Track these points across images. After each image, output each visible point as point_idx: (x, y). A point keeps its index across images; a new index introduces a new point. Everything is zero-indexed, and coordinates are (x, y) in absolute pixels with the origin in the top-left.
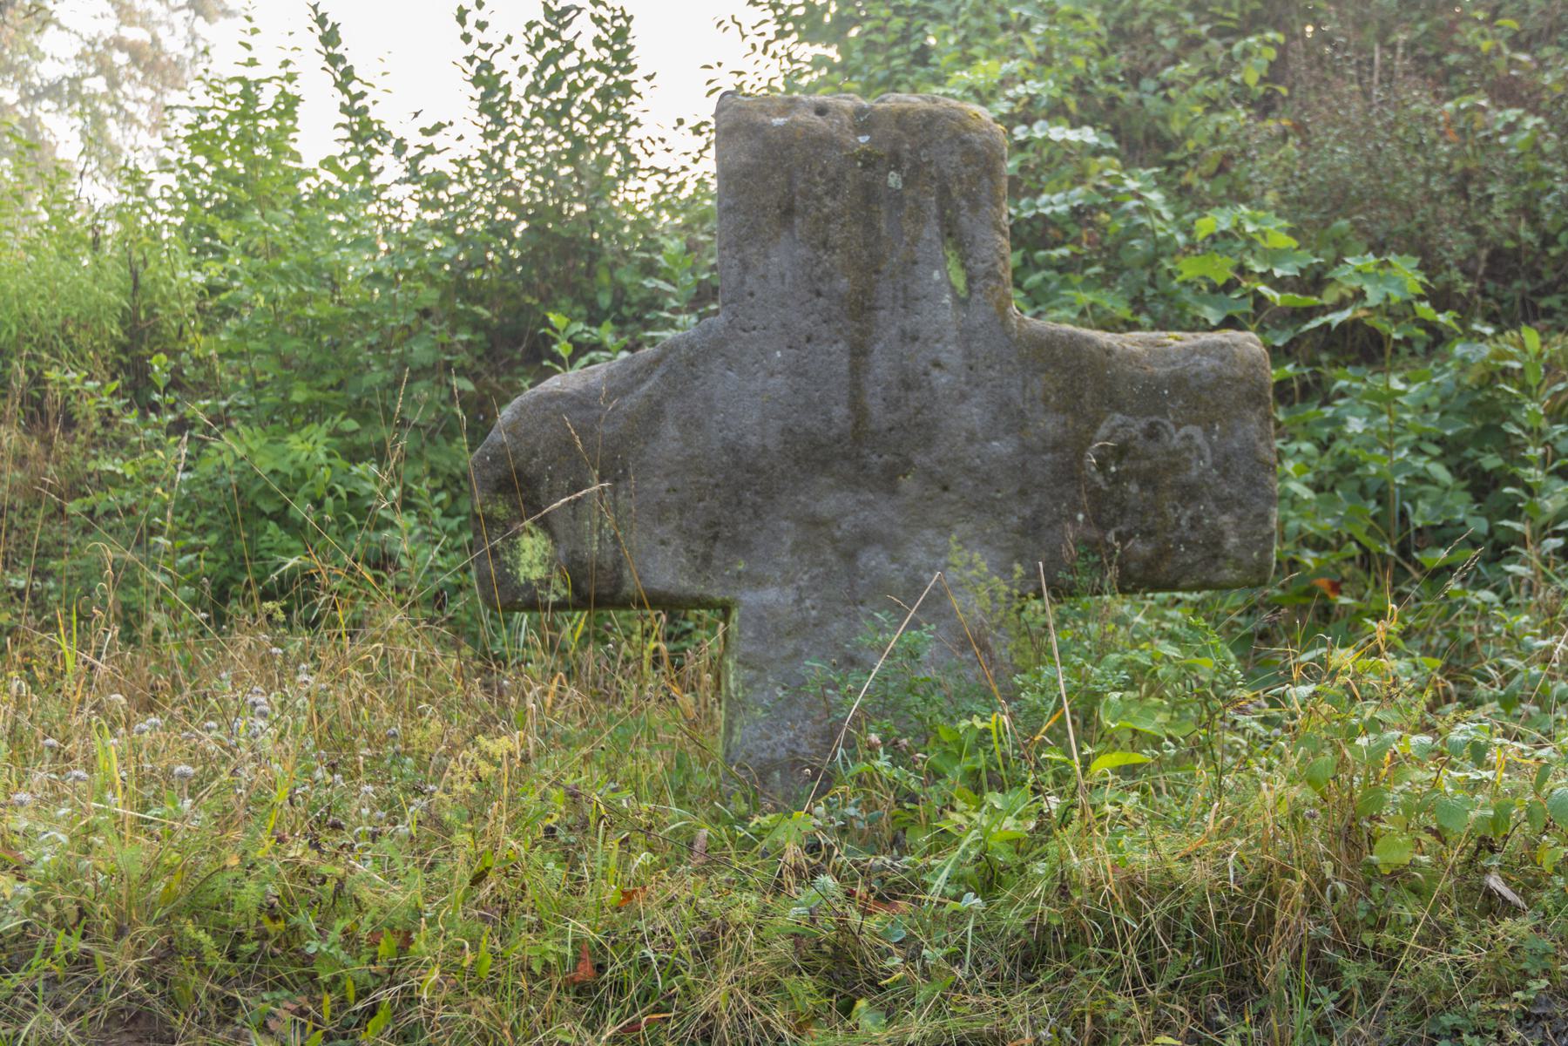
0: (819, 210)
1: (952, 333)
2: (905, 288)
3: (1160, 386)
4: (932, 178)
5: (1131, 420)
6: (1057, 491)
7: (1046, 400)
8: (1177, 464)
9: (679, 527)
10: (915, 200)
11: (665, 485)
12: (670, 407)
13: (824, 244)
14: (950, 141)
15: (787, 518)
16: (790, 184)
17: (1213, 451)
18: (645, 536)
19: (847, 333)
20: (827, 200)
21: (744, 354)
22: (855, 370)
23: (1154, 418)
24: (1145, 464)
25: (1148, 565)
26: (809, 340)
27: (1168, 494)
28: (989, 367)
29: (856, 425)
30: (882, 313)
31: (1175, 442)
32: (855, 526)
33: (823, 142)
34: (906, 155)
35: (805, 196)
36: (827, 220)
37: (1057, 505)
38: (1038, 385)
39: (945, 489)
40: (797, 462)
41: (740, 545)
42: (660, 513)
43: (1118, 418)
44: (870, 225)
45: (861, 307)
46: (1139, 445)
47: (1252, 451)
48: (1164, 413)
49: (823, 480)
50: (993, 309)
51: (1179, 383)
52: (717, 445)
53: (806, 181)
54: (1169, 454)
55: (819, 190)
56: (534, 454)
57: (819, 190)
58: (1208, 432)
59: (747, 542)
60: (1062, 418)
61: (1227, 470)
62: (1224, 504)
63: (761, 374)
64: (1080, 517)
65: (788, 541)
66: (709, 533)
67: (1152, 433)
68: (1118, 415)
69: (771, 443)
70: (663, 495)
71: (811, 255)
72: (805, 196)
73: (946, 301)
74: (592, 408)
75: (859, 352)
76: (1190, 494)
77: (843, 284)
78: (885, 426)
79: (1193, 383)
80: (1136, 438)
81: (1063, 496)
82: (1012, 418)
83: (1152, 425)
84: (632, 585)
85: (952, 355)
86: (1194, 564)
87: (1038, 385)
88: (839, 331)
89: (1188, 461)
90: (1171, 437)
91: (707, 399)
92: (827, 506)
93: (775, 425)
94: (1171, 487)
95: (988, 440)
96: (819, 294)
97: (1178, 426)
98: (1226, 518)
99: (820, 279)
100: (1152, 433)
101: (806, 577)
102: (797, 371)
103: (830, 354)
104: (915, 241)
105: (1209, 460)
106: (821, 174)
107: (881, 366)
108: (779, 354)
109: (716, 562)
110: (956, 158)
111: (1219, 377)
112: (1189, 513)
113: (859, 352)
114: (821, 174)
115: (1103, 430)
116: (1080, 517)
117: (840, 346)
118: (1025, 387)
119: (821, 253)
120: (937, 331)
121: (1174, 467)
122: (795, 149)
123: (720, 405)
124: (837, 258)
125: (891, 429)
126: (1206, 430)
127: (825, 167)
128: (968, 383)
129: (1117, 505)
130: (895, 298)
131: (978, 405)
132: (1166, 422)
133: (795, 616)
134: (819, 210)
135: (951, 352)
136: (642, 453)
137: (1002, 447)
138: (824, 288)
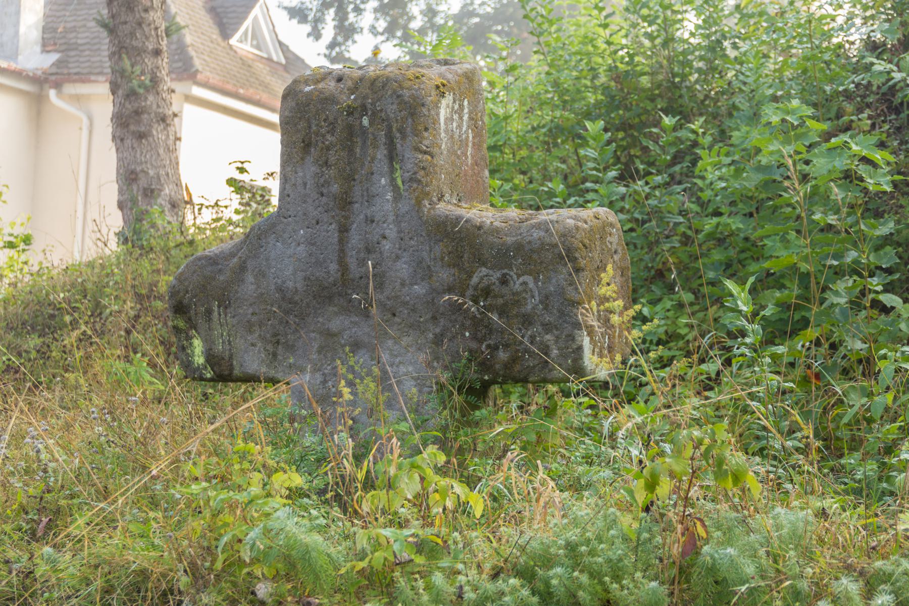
0: (323, 143)
1: (391, 218)
2: (367, 190)
3: (508, 250)
4: (383, 120)
5: (491, 272)
6: (453, 317)
7: (442, 259)
8: (518, 301)
9: (260, 335)
10: (373, 134)
11: (250, 311)
12: (250, 264)
13: (326, 163)
14: (391, 96)
15: (314, 332)
16: (310, 127)
17: (540, 293)
18: (242, 341)
19: (337, 218)
20: (329, 137)
21: (284, 232)
22: (342, 241)
23: (505, 271)
24: (500, 301)
25: (507, 366)
26: (318, 223)
27: (515, 321)
28: (411, 239)
29: (343, 275)
30: (356, 205)
31: (517, 286)
32: (351, 337)
33: (328, 100)
34: (369, 106)
35: (317, 134)
36: (328, 149)
37: (454, 326)
38: (438, 249)
39: (394, 315)
40: (314, 297)
41: (290, 348)
42: (249, 327)
43: (484, 271)
44: (351, 151)
45: (345, 202)
46: (496, 288)
47: (562, 293)
48: (511, 269)
49: (331, 309)
50: (413, 201)
51: (519, 247)
52: (273, 287)
53: (317, 125)
54: (514, 294)
55: (323, 131)
56: (187, 292)
57: (323, 131)
58: (536, 280)
59: (293, 346)
60: (452, 271)
61: (547, 305)
62: (548, 328)
63: (293, 244)
64: (467, 334)
65: (316, 346)
66: (274, 340)
67: (504, 281)
68: (484, 269)
69: (299, 286)
70: (249, 316)
71: (318, 171)
72: (317, 134)
73: (388, 197)
74: (218, 264)
75: (344, 230)
76: (527, 321)
77: (335, 188)
78: (358, 276)
79: (527, 248)
80: (494, 284)
81: (456, 320)
82: (423, 272)
83: (504, 275)
84: (237, 372)
85: (391, 232)
86: (534, 367)
87: (438, 249)
88: (333, 217)
89: (525, 298)
90: (515, 283)
91: (267, 260)
92: (335, 324)
93: (300, 275)
94: (517, 316)
95: (412, 284)
96: (322, 195)
97: (519, 276)
98: (548, 337)
99: (323, 186)
100: (504, 281)
101: (329, 368)
102: (311, 242)
103: (328, 232)
104: (373, 159)
105: (537, 298)
106: (325, 120)
107: (355, 239)
108: (302, 232)
109: (280, 357)
110: (395, 107)
111: (543, 244)
112: (529, 333)
113: (344, 230)
114: (325, 120)
115: (475, 280)
116: (467, 334)
117: (333, 226)
118: (431, 251)
119: (324, 169)
120: (384, 216)
121: (518, 303)
122: (312, 106)
123: (274, 263)
124: (333, 172)
125: (361, 278)
126: (535, 279)
127: (327, 116)
128: (400, 249)
129: (486, 327)
130: (362, 195)
131: (405, 263)
132: (512, 273)
133: (321, 391)
134: (323, 143)
135: (391, 229)
136: (237, 292)
137: (419, 289)
138: (325, 191)
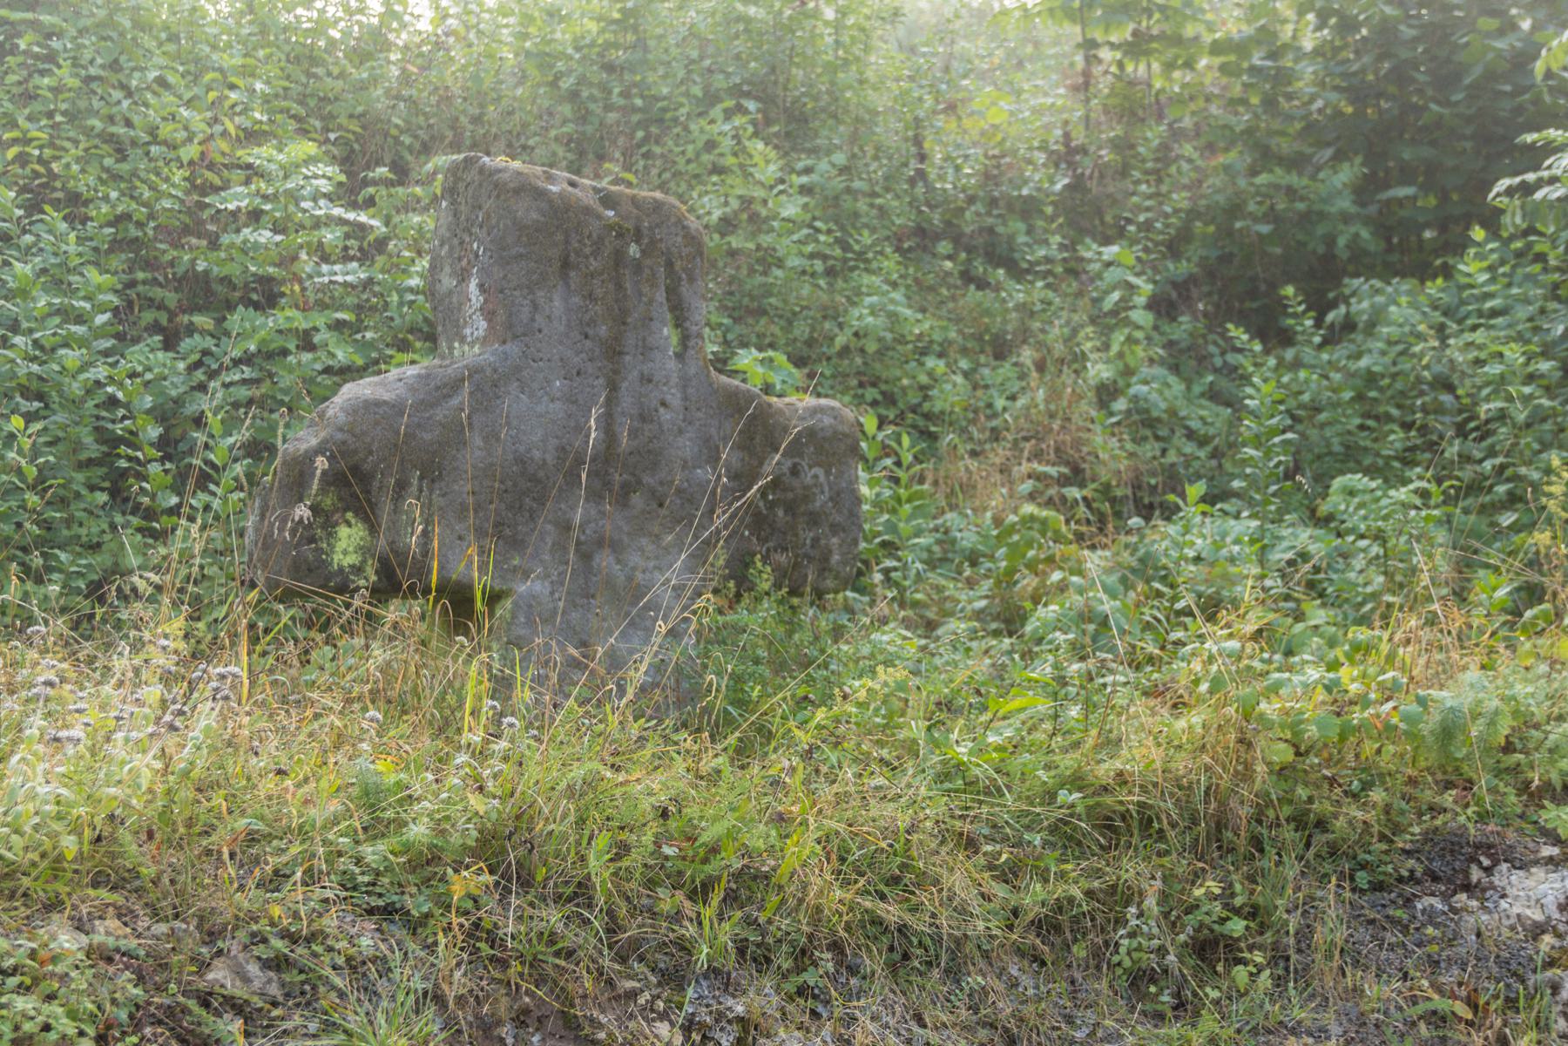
1: (674, 380)
2: (644, 340)
16: (567, 242)
23: (797, 460)
24: (790, 495)
26: (578, 373)
29: (608, 448)
30: (628, 358)
34: (646, 232)
35: (578, 254)
45: (613, 351)
46: (787, 479)
52: (511, 457)
55: (587, 250)
56: (371, 453)
58: (828, 473)
59: (523, 541)
62: (835, 529)
67: (795, 471)
69: (549, 458)
76: (814, 520)
83: (795, 465)
85: (675, 399)
95: (695, 468)
96: (586, 337)
97: (811, 467)
98: (835, 540)
104: (651, 301)
107: (626, 402)
114: (589, 237)
121: (807, 498)
131: (690, 439)
138: (591, 332)
